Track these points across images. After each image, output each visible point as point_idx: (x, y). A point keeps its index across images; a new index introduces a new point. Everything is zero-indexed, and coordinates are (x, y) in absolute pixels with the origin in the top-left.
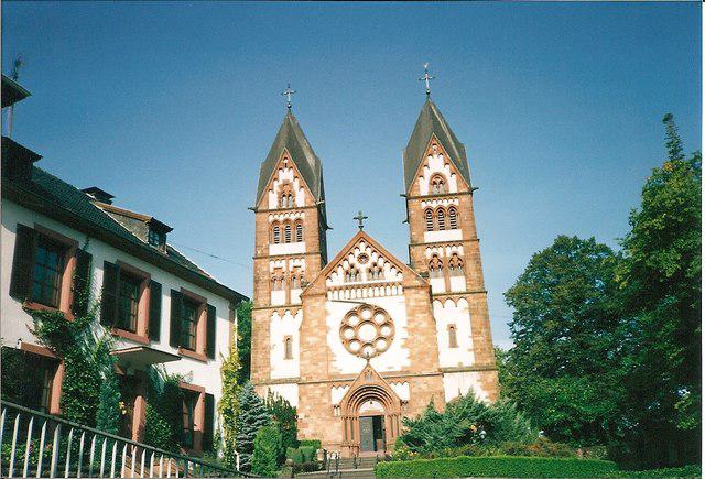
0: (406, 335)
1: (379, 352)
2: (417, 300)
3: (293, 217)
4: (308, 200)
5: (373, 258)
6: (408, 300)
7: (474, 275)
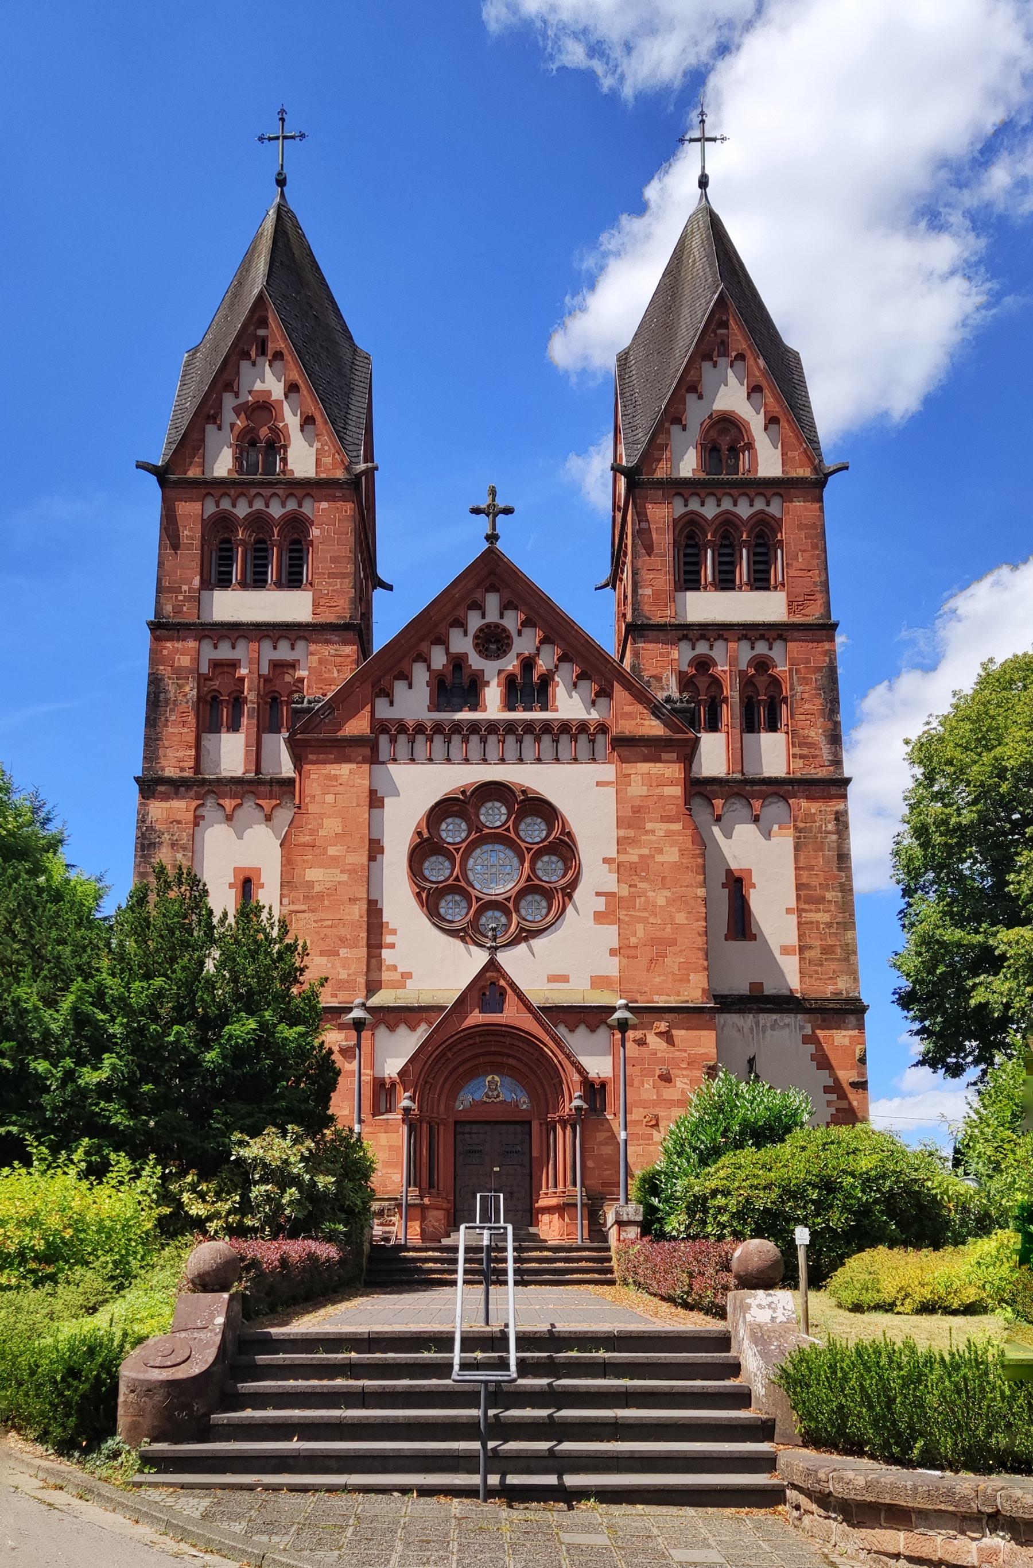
0: (610, 882)
3: (276, 511)
4: (327, 460)
5: (525, 643)
6: (622, 781)
7: (816, 734)
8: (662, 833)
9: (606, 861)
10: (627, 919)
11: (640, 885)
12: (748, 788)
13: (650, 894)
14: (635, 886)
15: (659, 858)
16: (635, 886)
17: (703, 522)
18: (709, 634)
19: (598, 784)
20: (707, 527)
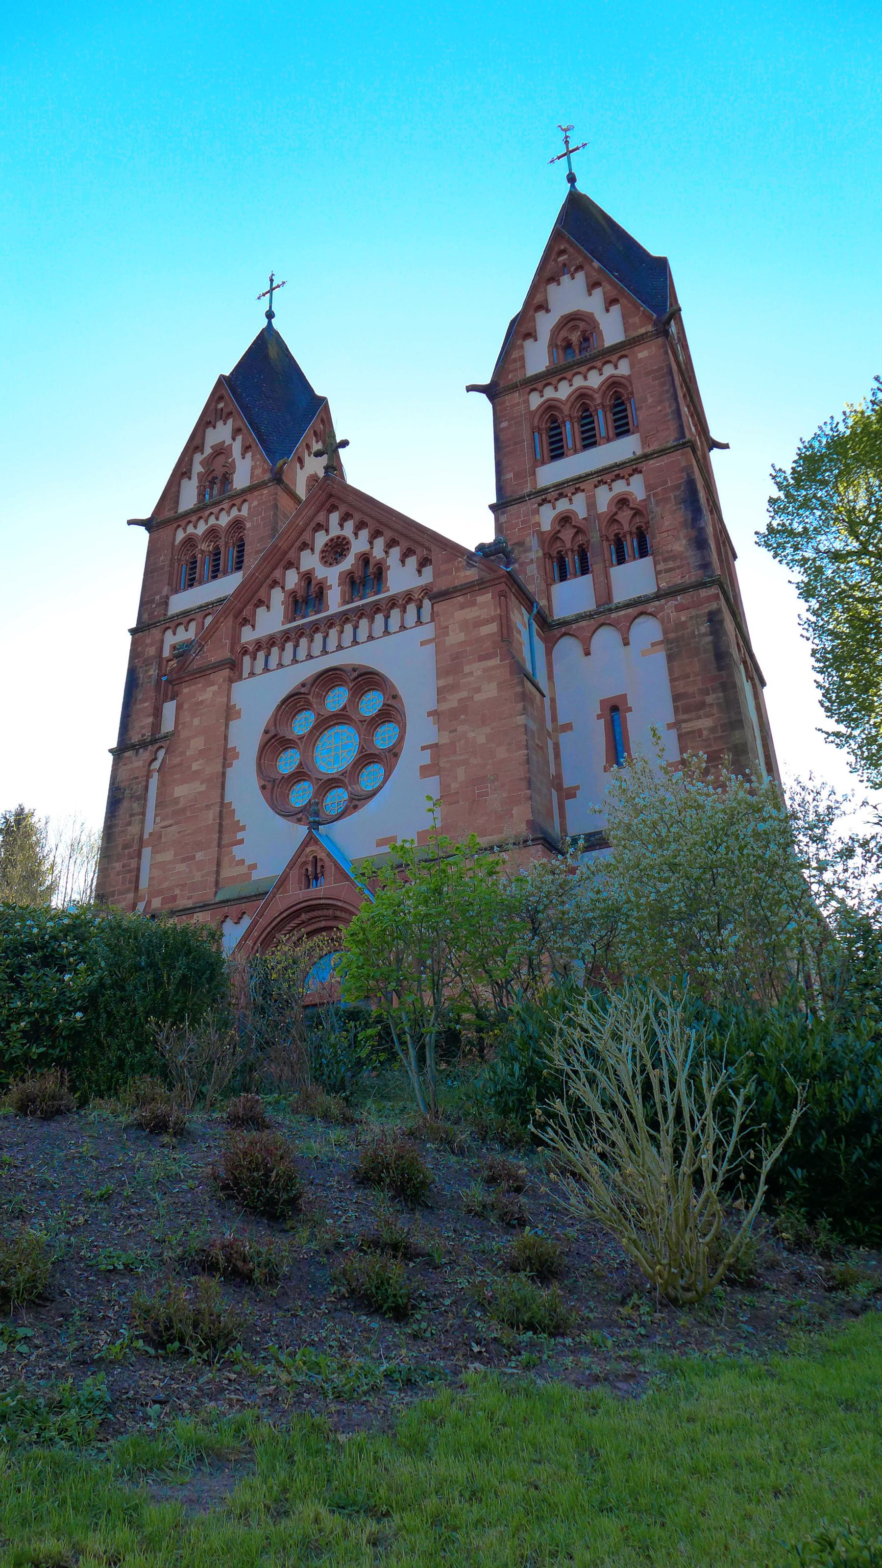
1: (357, 802)
2: (465, 626)
8: (479, 673)
9: (430, 714)
10: (448, 765)
11: (460, 729)
12: (613, 615)
13: (471, 735)
14: (455, 730)
15: (478, 697)
16: (455, 730)
17: (558, 404)
18: (565, 491)
19: (423, 643)
20: (562, 406)
